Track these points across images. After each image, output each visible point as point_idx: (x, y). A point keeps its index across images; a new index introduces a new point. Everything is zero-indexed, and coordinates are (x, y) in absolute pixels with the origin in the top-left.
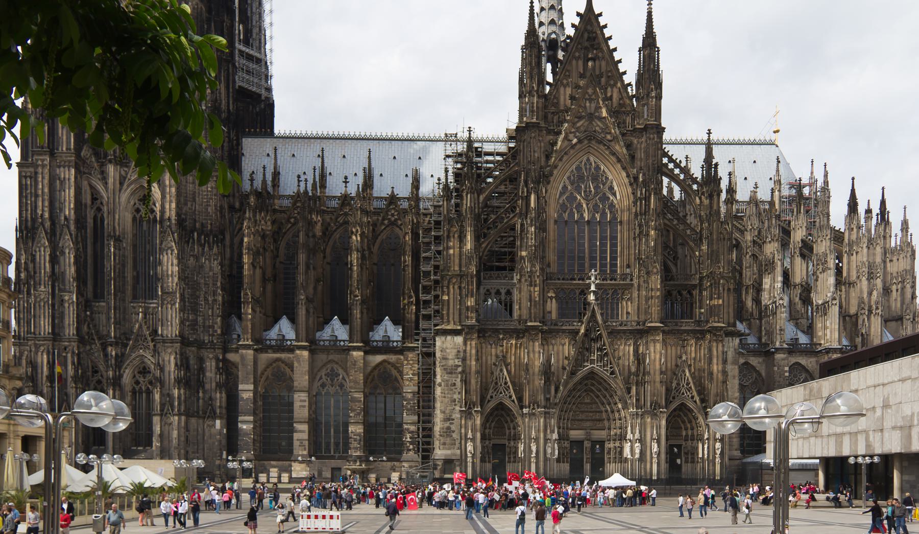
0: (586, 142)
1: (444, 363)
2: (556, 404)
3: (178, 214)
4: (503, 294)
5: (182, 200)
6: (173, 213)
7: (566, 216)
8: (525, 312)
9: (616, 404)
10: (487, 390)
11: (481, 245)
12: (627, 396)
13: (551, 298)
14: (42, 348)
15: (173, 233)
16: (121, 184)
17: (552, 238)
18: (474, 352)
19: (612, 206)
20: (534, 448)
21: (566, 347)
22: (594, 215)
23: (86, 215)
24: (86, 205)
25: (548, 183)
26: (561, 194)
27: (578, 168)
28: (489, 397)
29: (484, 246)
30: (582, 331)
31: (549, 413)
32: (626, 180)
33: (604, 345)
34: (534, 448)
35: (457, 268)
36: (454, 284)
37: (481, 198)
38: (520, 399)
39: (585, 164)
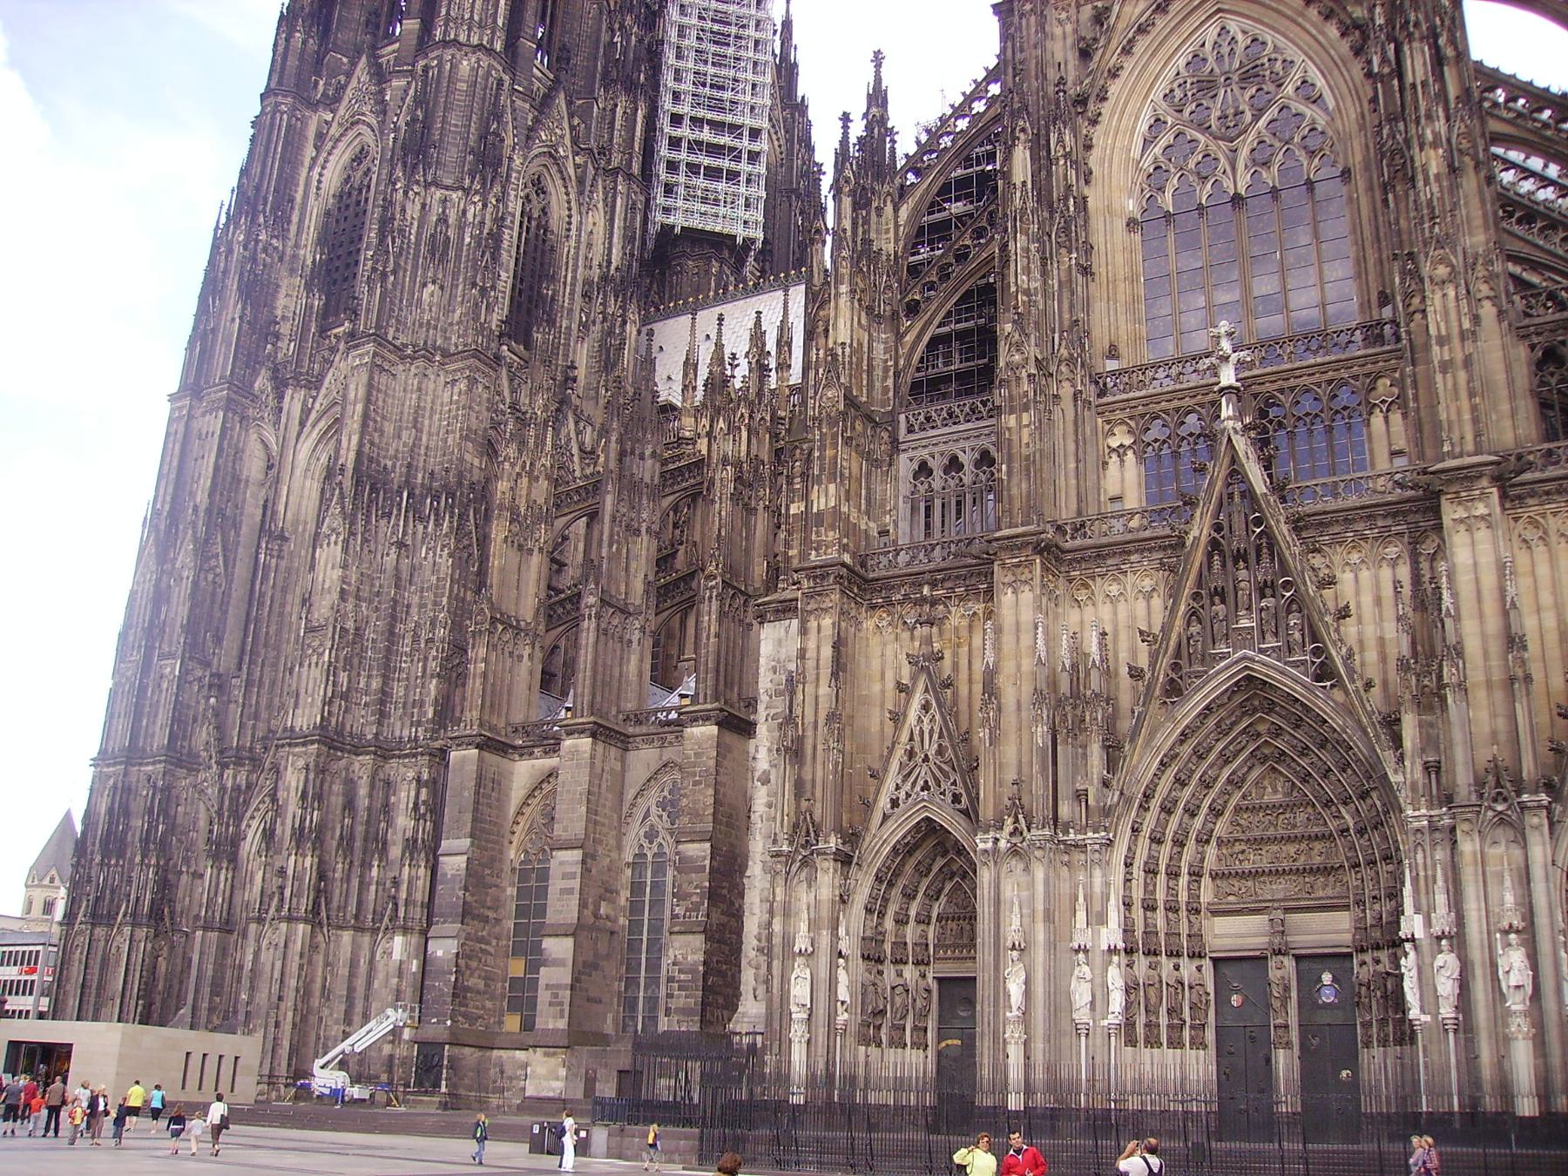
2: (1107, 812)
4: (968, 467)
6: (352, 455)
7: (1167, 201)
9: (1364, 796)
10: (877, 776)
11: (899, 337)
12: (1388, 757)
13: (1120, 451)
16: (302, 424)
18: (827, 652)
20: (1015, 989)
21: (1157, 602)
23: (244, 501)
25: (1094, 122)
26: (1147, 143)
27: (1197, 59)
28: (884, 802)
29: (909, 338)
31: (1081, 847)
32: (1344, 47)
33: (1285, 571)
34: (1015, 989)
37: (904, 212)
38: (974, 799)
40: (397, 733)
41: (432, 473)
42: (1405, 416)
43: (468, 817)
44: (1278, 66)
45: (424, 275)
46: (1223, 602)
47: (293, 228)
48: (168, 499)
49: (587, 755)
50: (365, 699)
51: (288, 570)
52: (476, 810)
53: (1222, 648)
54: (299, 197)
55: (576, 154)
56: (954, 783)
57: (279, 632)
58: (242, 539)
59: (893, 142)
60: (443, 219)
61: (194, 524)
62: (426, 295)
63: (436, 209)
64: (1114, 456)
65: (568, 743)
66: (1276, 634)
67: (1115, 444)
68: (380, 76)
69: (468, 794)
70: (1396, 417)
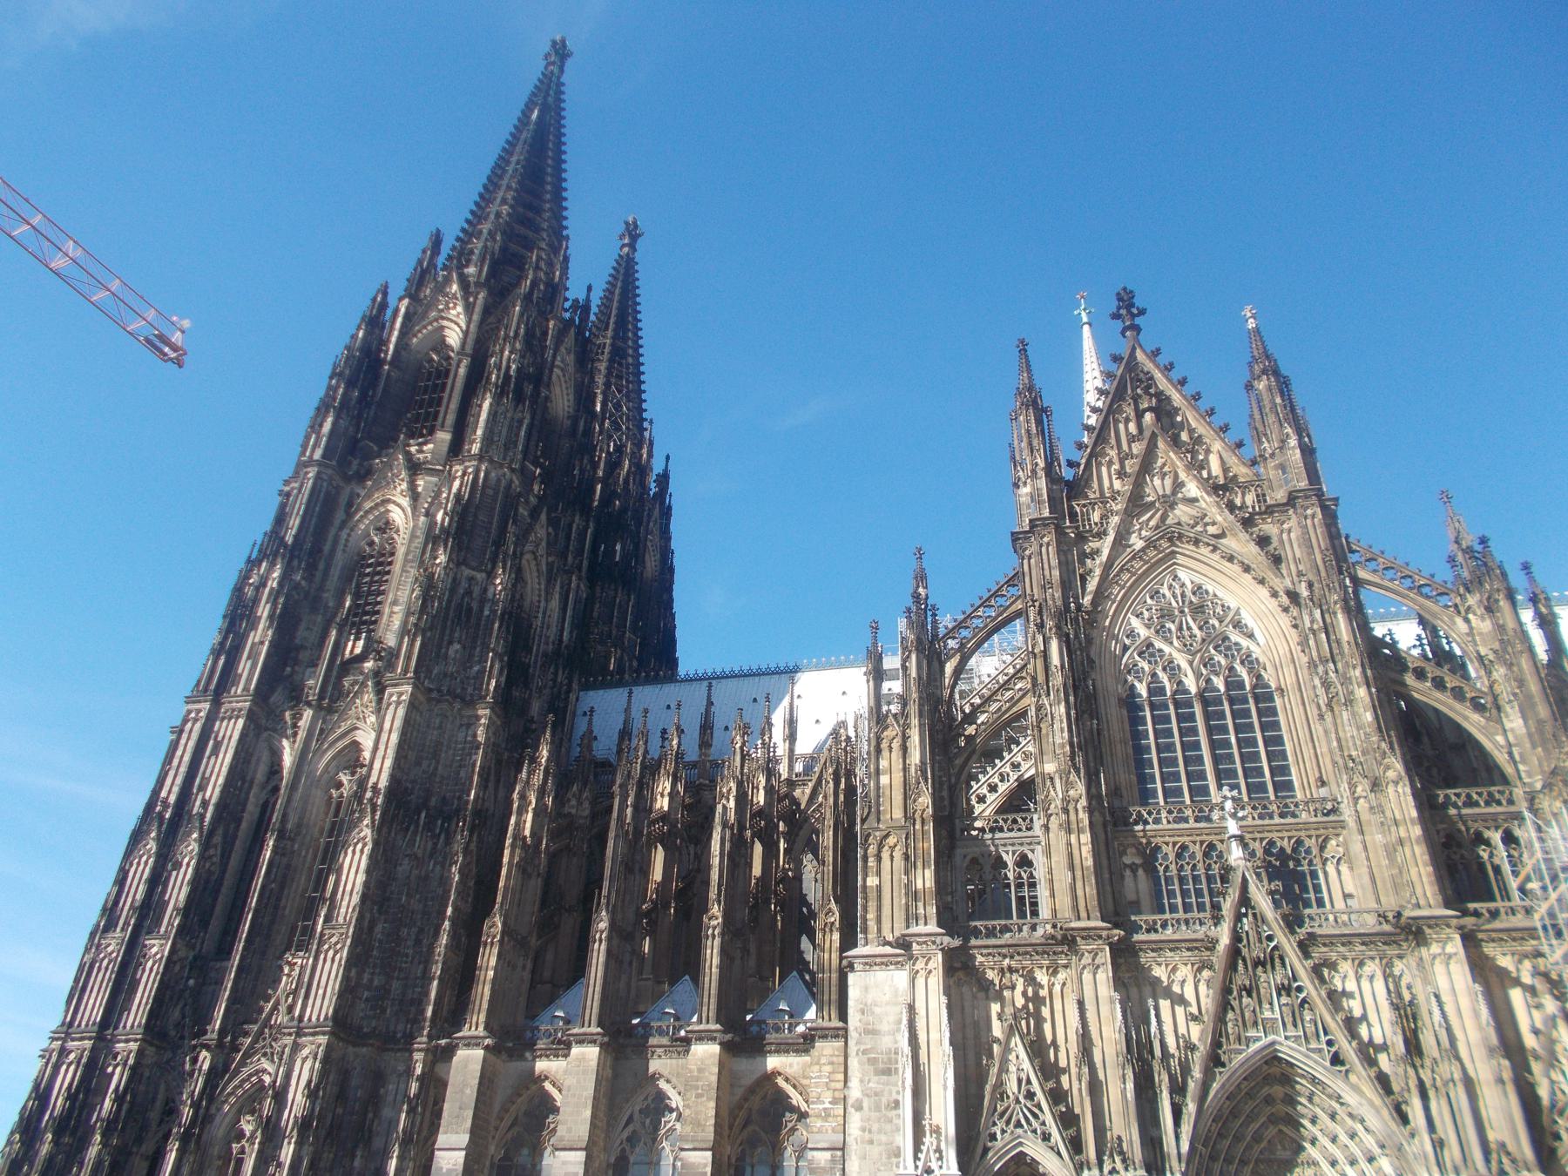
0: (1165, 544)
1: (868, 1043)
3: (394, 779)
5: (412, 756)
8: (1064, 902)
11: (950, 760)
13: (1133, 868)
14: (72, 1056)
15: (374, 812)
17: (1118, 736)
19: (1248, 660)
22: (1208, 681)
23: (247, 799)
24: (252, 782)
30: (1225, 940)
35: (898, 814)
36: (892, 848)
39: (1170, 587)
40: (392, 1028)
41: (444, 798)
42: (1351, 869)
43: (470, 1113)
44: (1219, 609)
45: (451, 635)
46: (1249, 995)
47: (319, 575)
48: (176, 789)
49: (594, 1064)
50: (366, 994)
51: (288, 866)
52: (476, 1107)
53: (1251, 1033)
54: (327, 548)
55: (549, 554)
56: (1043, 1123)
57: (272, 922)
58: (241, 834)
59: (934, 615)
60: (469, 592)
61: (202, 816)
62: (451, 652)
63: (464, 584)
64: (1128, 873)
65: (576, 1050)
66: (1295, 1026)
67: (1127, 860)
68: (414, 468)
69: (471, 1092)
70: (1344, 868)
